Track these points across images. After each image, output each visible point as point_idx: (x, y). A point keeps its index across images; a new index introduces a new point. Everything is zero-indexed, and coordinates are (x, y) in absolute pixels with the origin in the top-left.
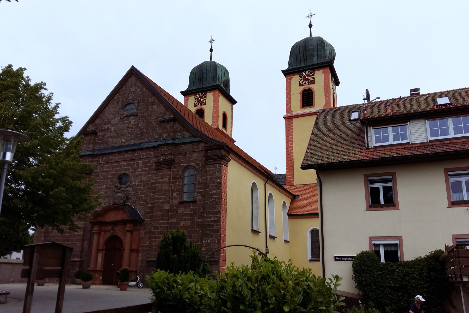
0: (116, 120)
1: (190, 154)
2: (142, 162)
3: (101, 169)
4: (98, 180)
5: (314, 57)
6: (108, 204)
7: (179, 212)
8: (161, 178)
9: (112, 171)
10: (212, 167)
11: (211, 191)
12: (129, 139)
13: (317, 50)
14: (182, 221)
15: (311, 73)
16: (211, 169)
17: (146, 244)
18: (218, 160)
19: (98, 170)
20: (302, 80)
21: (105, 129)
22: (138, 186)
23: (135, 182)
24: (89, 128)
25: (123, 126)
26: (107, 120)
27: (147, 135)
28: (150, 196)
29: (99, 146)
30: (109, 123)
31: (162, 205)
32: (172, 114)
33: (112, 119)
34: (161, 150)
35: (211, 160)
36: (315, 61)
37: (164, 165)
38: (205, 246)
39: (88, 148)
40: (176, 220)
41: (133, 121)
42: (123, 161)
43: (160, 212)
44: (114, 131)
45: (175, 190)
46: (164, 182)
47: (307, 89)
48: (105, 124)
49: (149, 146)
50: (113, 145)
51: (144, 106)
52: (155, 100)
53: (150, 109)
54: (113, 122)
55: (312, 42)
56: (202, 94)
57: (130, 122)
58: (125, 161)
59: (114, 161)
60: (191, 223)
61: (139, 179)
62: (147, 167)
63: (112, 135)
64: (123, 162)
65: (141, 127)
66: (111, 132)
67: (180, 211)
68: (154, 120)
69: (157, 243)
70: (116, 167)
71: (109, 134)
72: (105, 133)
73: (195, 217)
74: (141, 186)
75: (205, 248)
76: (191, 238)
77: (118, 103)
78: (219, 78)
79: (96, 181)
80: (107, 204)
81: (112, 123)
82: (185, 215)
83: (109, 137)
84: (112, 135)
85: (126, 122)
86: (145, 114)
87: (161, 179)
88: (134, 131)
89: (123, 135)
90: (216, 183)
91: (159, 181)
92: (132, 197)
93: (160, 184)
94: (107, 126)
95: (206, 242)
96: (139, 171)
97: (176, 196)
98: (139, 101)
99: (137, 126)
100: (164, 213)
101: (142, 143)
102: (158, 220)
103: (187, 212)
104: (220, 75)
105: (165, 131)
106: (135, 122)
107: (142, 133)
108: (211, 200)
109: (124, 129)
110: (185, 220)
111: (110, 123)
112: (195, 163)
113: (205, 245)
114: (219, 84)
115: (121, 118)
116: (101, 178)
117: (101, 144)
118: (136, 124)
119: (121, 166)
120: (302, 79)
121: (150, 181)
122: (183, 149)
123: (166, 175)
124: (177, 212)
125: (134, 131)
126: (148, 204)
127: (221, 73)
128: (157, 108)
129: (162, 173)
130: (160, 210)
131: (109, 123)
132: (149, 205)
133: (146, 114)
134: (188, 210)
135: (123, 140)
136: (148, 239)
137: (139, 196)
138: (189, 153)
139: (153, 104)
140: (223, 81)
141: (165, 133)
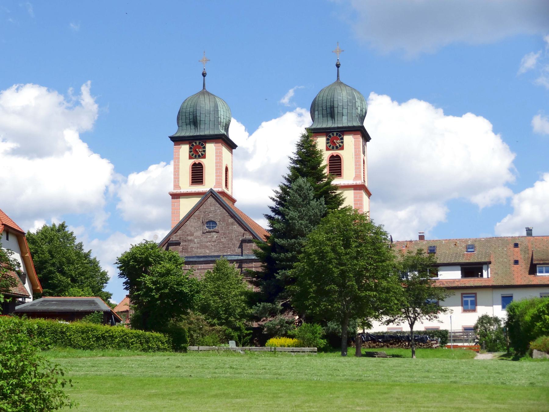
0: (199, 233)
5: (343, 115)
13: (346, 107)
15: (340, 136)
20: (329, 143)
24: (173, 238)
25: (205, 240)
26: (189, 233)
27: (229, 249)
30: (192, 235)
33: (195, 232)
36: (344, 122)
41: (215, 237)
44: (198, 243)
47: (335, 155)
48: (188, 235)
49: (233, 259)
50: (198, 255)
51: (224, 225)
53: (230, 228)
54: (195, 234)
55: (341, 97)
56: (199, 143)
57: (213, 237)
63: (195, 245)
65: (223, 242)
66: (195, 243)
71: (192, 245)
77: (199, 218)
78: (221, 122)
83: (193, 247)
84: (195, 245)
85: (209, 236)
88: (217, 245)
89: (207, 247)
94: (189, 238)
101: (226, 255)
104: (222, 117)
106: (217, 237)
107: (224, 247)
111: (193, 236)
114: (224, 135)
115: (203, 233)
118: (219, 239)
120: (329, 141)
125: (217, 245)
127: (222, 113)
131: (192, 235)
133: (227, 232)
135: (208, 251)
139: (232, 224)
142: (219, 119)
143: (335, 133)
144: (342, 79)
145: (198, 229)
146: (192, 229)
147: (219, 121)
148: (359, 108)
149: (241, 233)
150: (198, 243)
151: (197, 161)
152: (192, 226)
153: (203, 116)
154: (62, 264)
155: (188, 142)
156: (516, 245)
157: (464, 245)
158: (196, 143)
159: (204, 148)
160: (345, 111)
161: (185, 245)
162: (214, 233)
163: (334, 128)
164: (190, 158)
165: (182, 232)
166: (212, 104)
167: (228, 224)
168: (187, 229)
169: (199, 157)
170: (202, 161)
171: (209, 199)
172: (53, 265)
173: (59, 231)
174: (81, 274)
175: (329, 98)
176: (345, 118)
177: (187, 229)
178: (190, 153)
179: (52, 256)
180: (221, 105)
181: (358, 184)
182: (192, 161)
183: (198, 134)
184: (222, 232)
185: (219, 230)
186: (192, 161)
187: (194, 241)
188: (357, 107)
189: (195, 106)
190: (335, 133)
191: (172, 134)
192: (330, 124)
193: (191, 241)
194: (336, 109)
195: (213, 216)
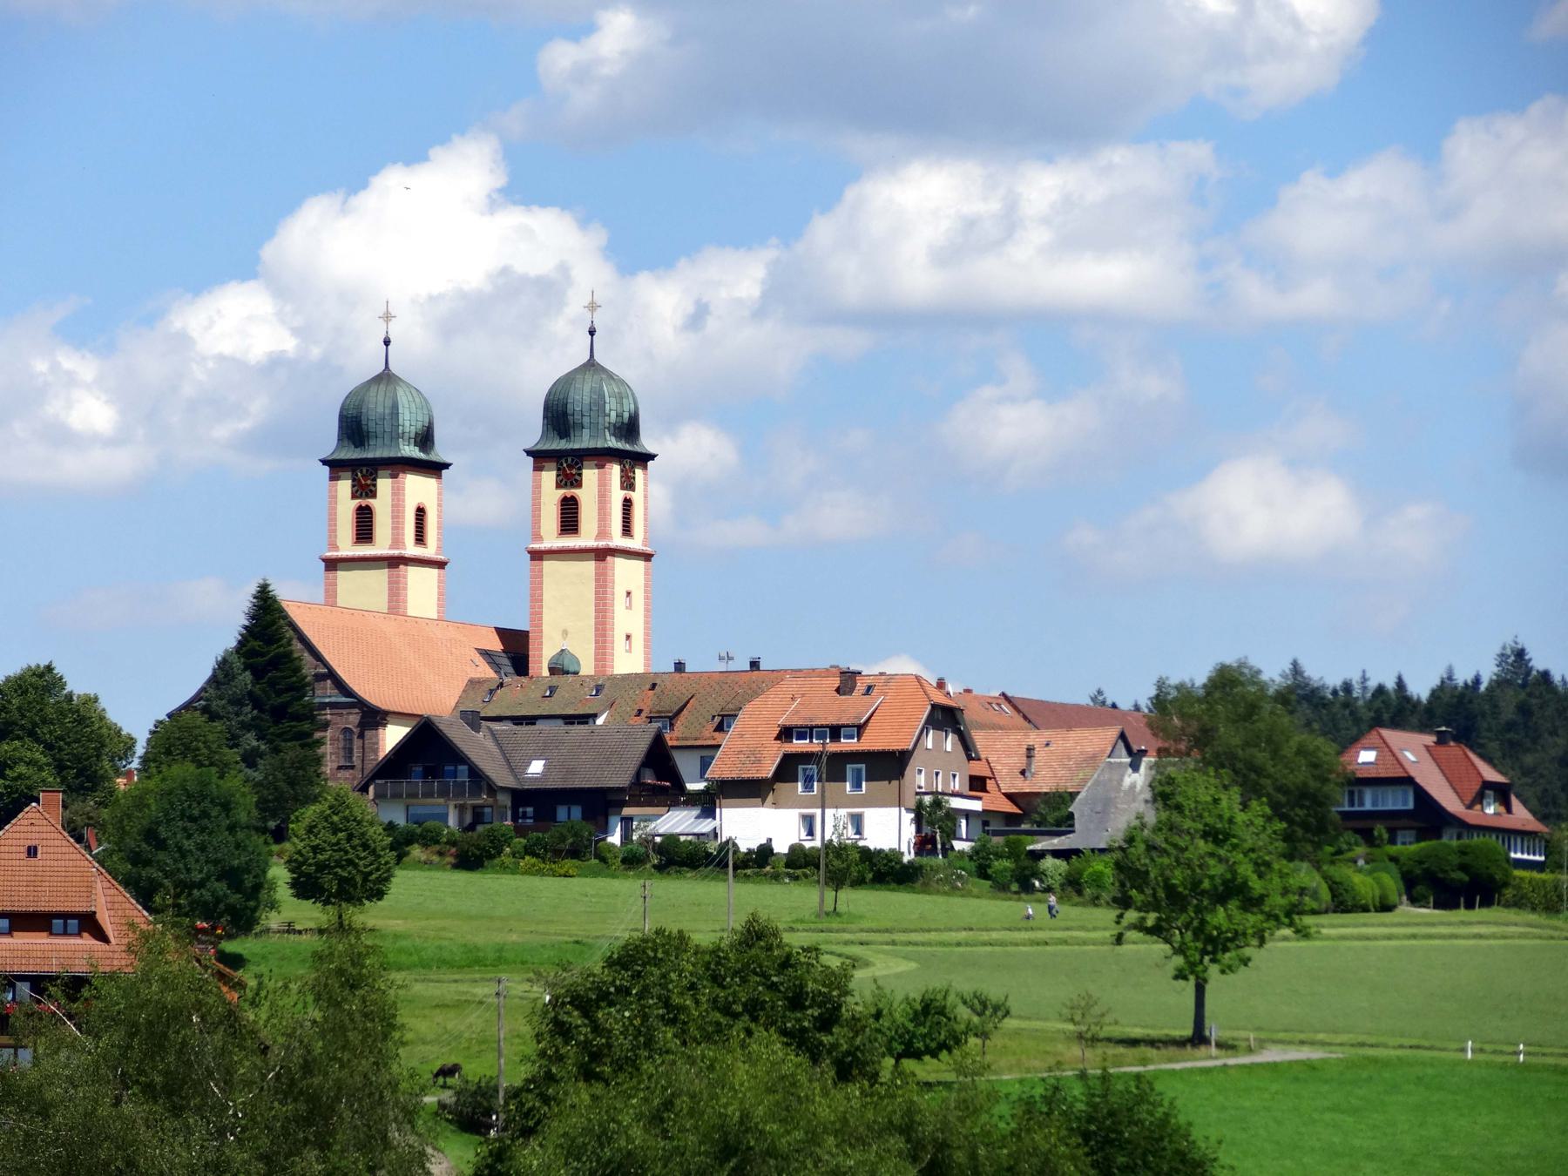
5: (583, 428)
15: (577, 463)
16: (368, 734)
104: (407, 424)
127: (407, 417)
140: (413, 435)
142: (401, 428)
143: (570, 460)
144: (596, 357)
147: (400, 431)
148: (613, 414)
151: (364, 502)
153: (372, 425)
154: (35, 725)
156: (654, 686)
157: (593, 684)
160: (586, 420)
163: (566, 450)
164: (354, 497)
166: (389, 403)
169: (367, 496)
170: (371, 502)
172: (22, 727)
173: (41, 675)
174: (61, 738)
175: (561, 397)
176: (586, 432)
179: (23, 716)
180: (404, 399)
181: (600, 546)
182: (356, 502)
183: (364, 456)
188: (607, 411)
189: (359, 407)
190: (570, 460)
191: (323, 456)
192: (562, 445)
194: (570, 418)
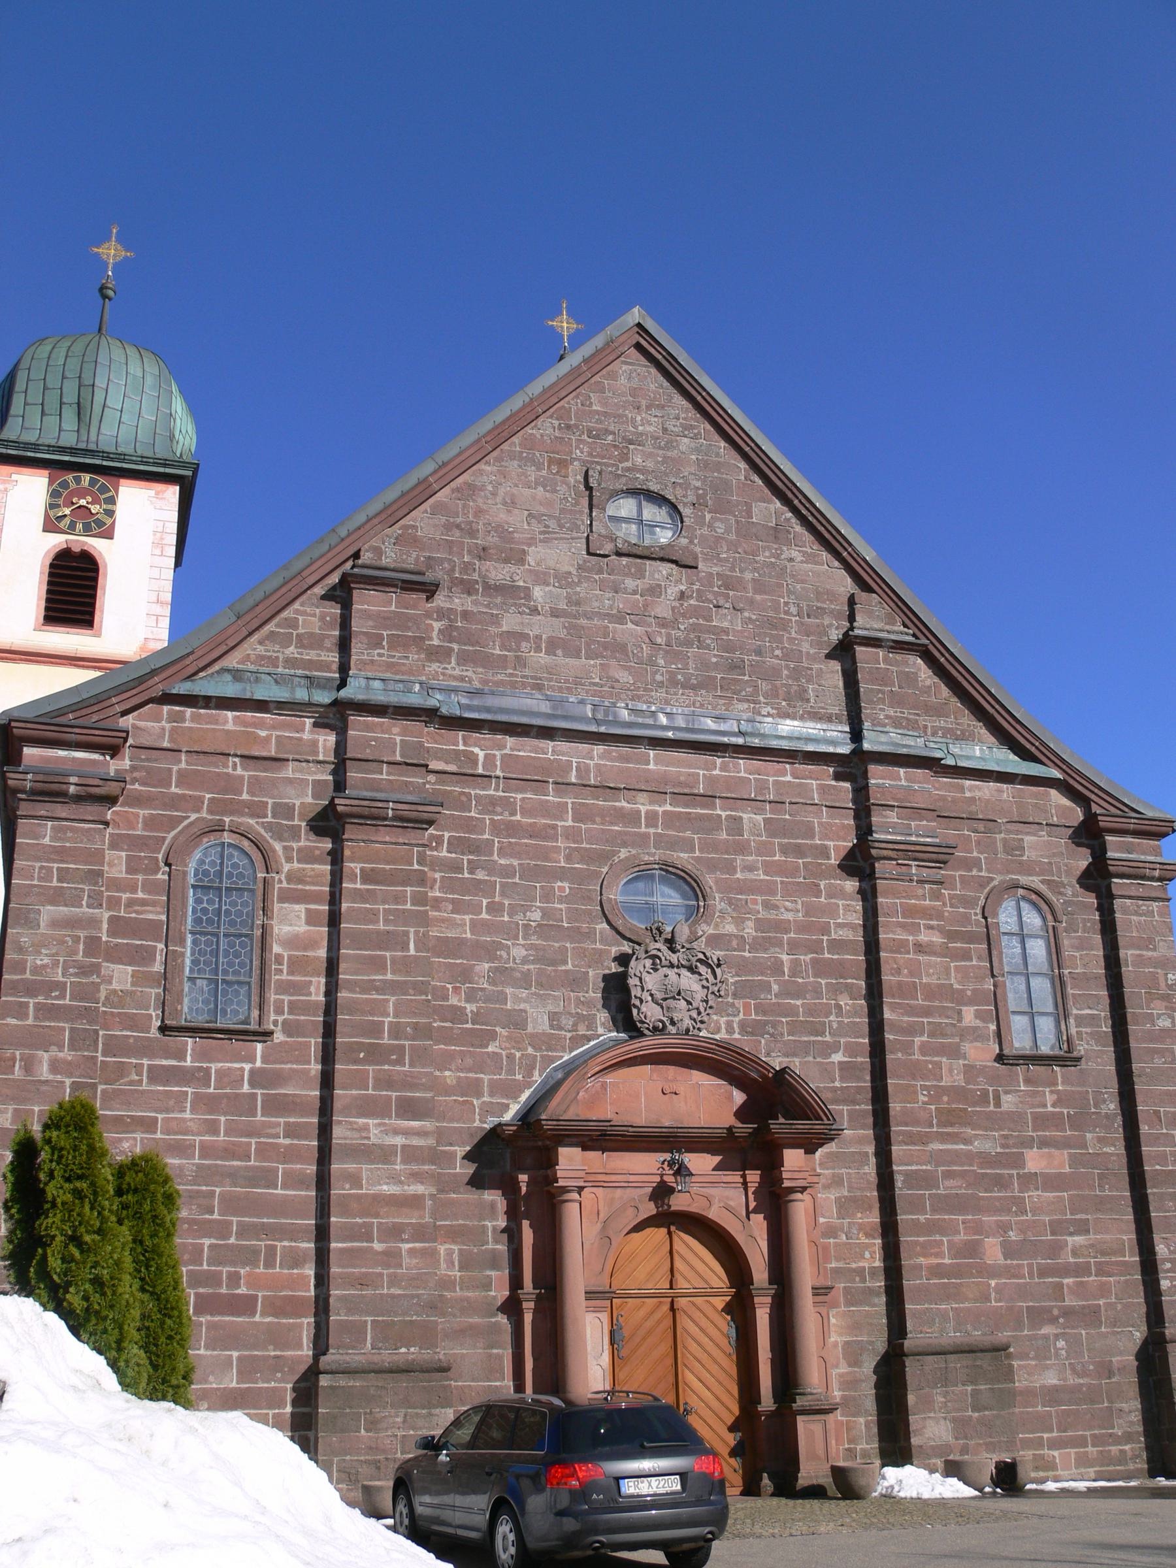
1: (1009, 832)
2: (759, 818)
3: (494, 813)
4: (481, 875)
6: (575, 1025)
7: (1005, 1107)
8: (903, 926)
9: (571, 834)
10: (1136, 913)
11: (1151, 1018)
12: (658, 678)
14: (1032, 1148)
17: (861, 1264)
18: (1155, 884)
19: (472, 814)
21: (487, 587)
22: (756, 945)
23: (739, 921)
24: (378, 552)
25: (607, 601)
26: (492, 540)
28: (839, 1007)
29: (457, 672)
31: (931, 1062)
32: (898, 619)
33: (531, 542)
34: (881, 781)
35: (1128, 881)
37: (910, 862)
38: (1168, 1271)
39: (390, 666)
40: (1003, 1146)
41: (673, 591)
42: (645, 794)
43: (926, 1099)
45: (969, 993)
46: (920, 948)
48: (483, 553)
51: (728, 531)
52: (788, 520)
54: (534, 555)
57: (655, 591)
58: (658, 794)
59: (578, 776)
60: (1074, 1161)
61: (760, 907)
62: (799, 851)
63: (541, 627)
64: (642, 797)
65: (725, 631)
66: (535, 611)
67: (1009, 1102)
68: (794, 619)
69: (939, 1255)
70: (598, 819)
71: (510, 622)
72: (488, 606)
73: (1089, 1136)
74: (777, 949)
75: (1172, 1279)
76: (1087, 1232)
77: (563, 464)
79: (466, 875)
80: (568, 1022)
81: (530, 559)
82: (1042, 1121)
83: (524, 637)
85: (630, 583)
86: (741, 571)
87: (899, 930)
89: (618, 649)
90: (1163, 984)
91: (891, 936)
92: (733, 1005)
93: (901, 953)
94: (499, 573)
95: (1169, 1249)
96: (750, 868)
97: (978, 1023)
98: (698, 497)
99: (701, 621)
100: (948, 1103)
102: (924, 1139)
103: (1045, 1106)
105: (883, 692)
106: (682, 596)
108: (1158, 1062)
109: (620, 618)
110: (1044, 1143)
111: (522, 561)
112: (1040, 878)
113: (1168, 1265)
116: (502, 862)
117: (464, 659)
119: (634, 818)
121: (825, 930)
122: (973, 799)
123: (925, 913)
124: (998, 1104)
126: (835, 1047)
128: (802, 562)
129: (904, 897)
130: (923, 1087)
132: (837, 1057)
133: (748, 576)
134: (1050, 1098)
136: (867, 1235)
137: (774, 1001)
138: (1009, 826)
141: (882, 701)
145: (553, 524)
146: (517, 521)
149: (832, 596)
150: (555, 613)
152: (511, 504)
155: (46, 472)
158: (78, 480)
159: (112, 501)
161: (466, 615)
162: (665, 568)
165: (448, 527)
167: (746, 531)
168: (479, 512)
171: (621, 369)
177: (479, 512)
178: (51, 513)
184: (715, 569)
185: (696, 558)
186: (57, 541)
187: (527, 593)
193: (508, 591)
195: (650, 464)
